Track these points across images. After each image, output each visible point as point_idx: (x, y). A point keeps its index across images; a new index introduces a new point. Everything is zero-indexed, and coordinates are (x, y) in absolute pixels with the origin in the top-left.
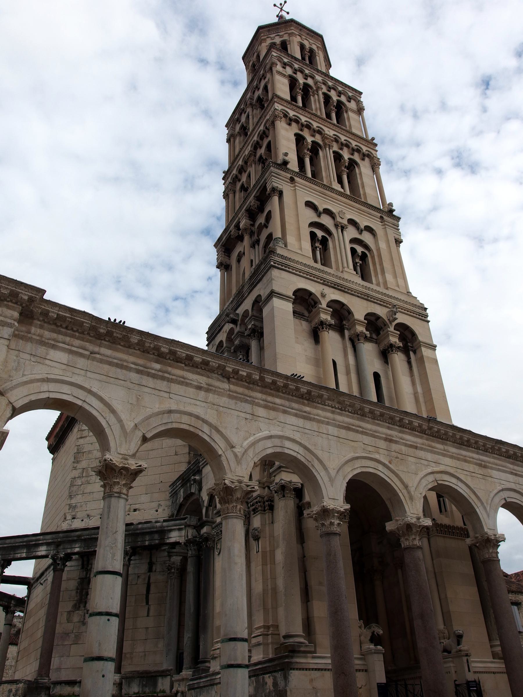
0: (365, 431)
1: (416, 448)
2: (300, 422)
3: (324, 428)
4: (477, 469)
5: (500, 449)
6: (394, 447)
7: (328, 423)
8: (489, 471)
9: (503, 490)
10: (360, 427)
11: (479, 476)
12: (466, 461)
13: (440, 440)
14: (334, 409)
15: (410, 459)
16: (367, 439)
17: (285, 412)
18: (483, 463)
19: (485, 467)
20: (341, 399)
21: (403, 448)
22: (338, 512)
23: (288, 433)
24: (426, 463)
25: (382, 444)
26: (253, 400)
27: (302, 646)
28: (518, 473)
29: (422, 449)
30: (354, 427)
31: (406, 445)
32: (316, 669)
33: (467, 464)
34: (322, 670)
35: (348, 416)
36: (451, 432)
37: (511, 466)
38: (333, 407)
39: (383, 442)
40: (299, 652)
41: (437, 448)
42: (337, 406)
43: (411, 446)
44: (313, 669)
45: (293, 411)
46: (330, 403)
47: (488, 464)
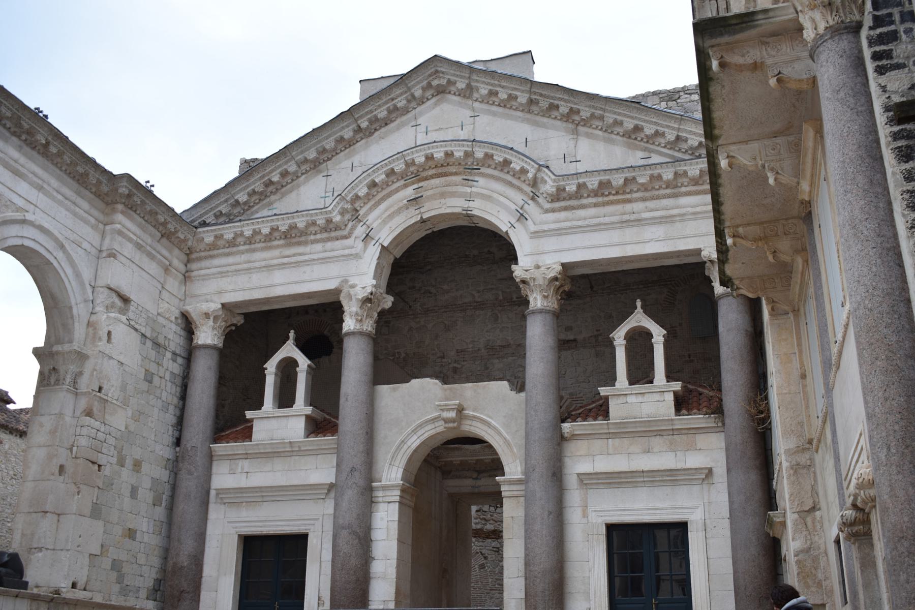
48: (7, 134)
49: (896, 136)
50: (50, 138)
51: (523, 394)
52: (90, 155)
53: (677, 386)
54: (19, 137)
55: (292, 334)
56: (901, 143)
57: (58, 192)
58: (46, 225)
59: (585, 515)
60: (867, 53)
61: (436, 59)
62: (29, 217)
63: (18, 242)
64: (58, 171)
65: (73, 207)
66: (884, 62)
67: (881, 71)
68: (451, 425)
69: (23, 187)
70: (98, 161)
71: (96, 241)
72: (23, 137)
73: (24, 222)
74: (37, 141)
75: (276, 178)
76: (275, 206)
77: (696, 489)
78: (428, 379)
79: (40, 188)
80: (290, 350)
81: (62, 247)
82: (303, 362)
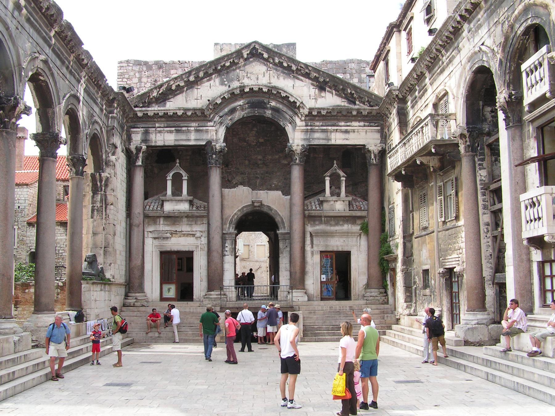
49: (482, 189)
51: (288, 197)
53: (350, 198)
55: (178, 161)
56: (483, 191)
59: (312, 247)
60: (478, 163)
61: (255, 42)
66: (481, 167)
67: (480, 169)
68: (258, 208)
71: (105, 121)
75: (174, 88)
76: (171, 100)
77: (355, 239)
78: (246, 188)
80: (178, 169)
81: (101, 129)
82: (185, 176)
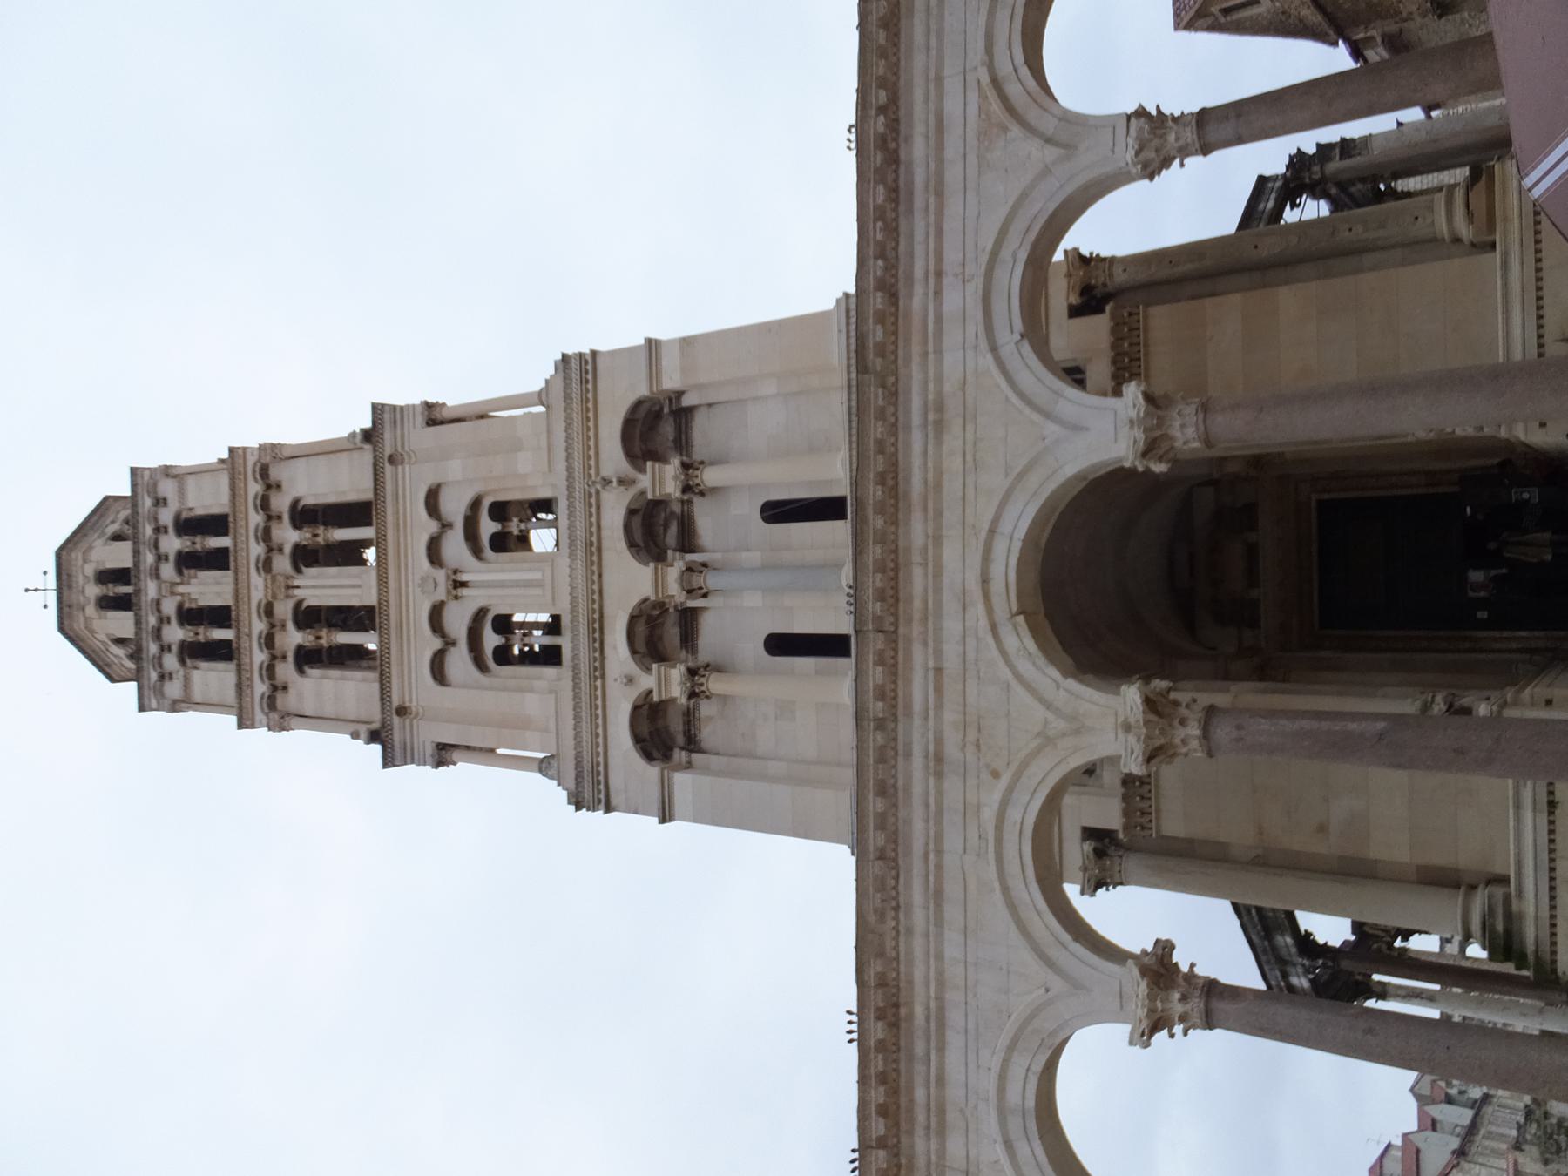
0: (932, 846)
1: (939, 671)
2: (954, 1041)
3: (954, 972)
4: (953, 441)
5: (881, 351)
6: (951, 750)
7: (940, 957)
8: (947, 388)
9: (994, 349)
10: (926, 855)
11: (970, 436)
12: (938, 486)
13: (901, 574)
14: (902, 930)
15: (971, 699)
16: (953, 841)
17: (941, 1081)
18: (931, 417)
19: (940, 408)
20: (872, 919)
21: (950, 716)
22: (1151, 997)
23: (989, 1084)
24: (971, 641)
25: (952, 785)
26: (933, 1167)
27: (1493, 926)
28: (932, 268)
29: (938, 653)
30: (931, 878)
31: (939, 706)
32: (1552, 898)
33: (946, 484)
34: (1552, 888)
35: (909, 886)
36: (874, 552)
37: (918, 289)
38: (898, 932)
39: (946, 785)
40: (1508, 932)
41: (926, 591)
42: (893, 923)
43: (939, 690)
44: (1553, 907)
45: (933, 1057)
46: (889, 944)
47: (931, 397)
48: (902, 170)
50: (873, 112)
52: (857, 34)
54: (896, 151)
57: (928, 49)
58: (981, 44)
62: (985, 79)
63: (1024, 71)
64: (903, 63)
65: (934, 11)
69: (953, 106)
70: (856, 21)
72: (893, 145)
73: (996, 82)
74: (887, 126)
79: (939, 80)
